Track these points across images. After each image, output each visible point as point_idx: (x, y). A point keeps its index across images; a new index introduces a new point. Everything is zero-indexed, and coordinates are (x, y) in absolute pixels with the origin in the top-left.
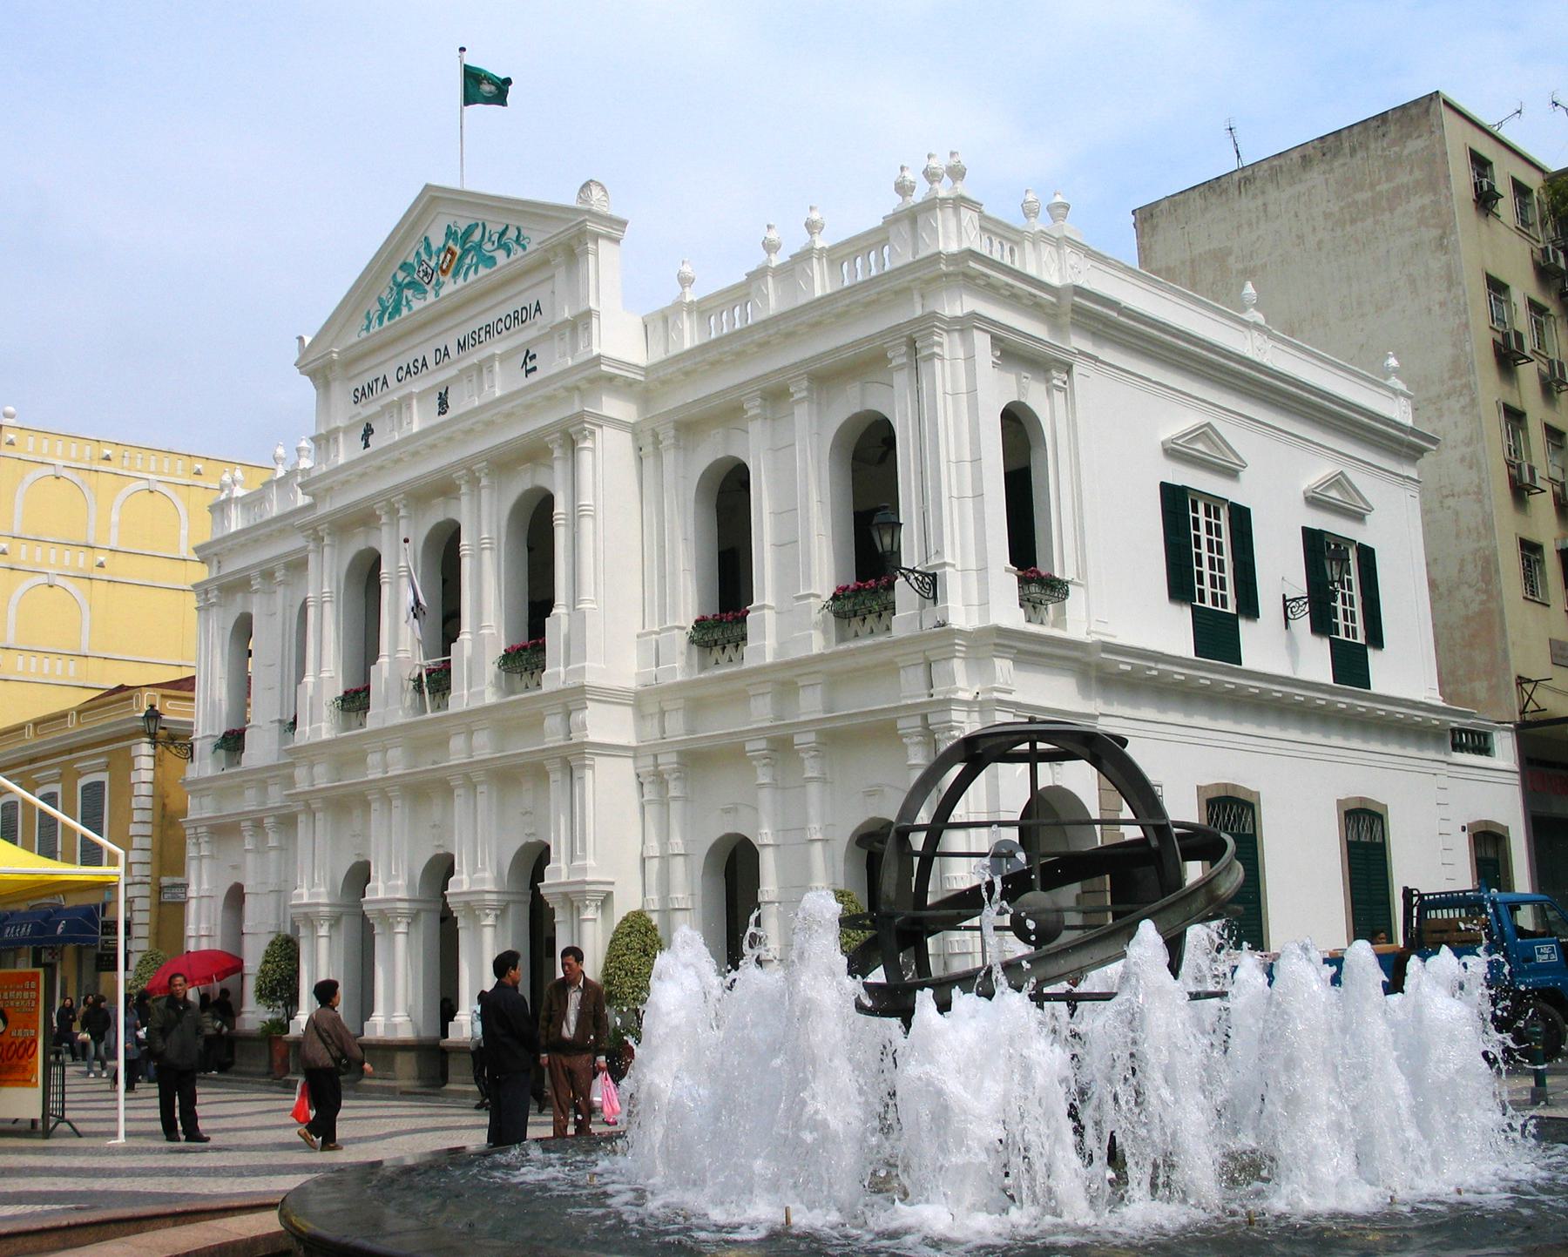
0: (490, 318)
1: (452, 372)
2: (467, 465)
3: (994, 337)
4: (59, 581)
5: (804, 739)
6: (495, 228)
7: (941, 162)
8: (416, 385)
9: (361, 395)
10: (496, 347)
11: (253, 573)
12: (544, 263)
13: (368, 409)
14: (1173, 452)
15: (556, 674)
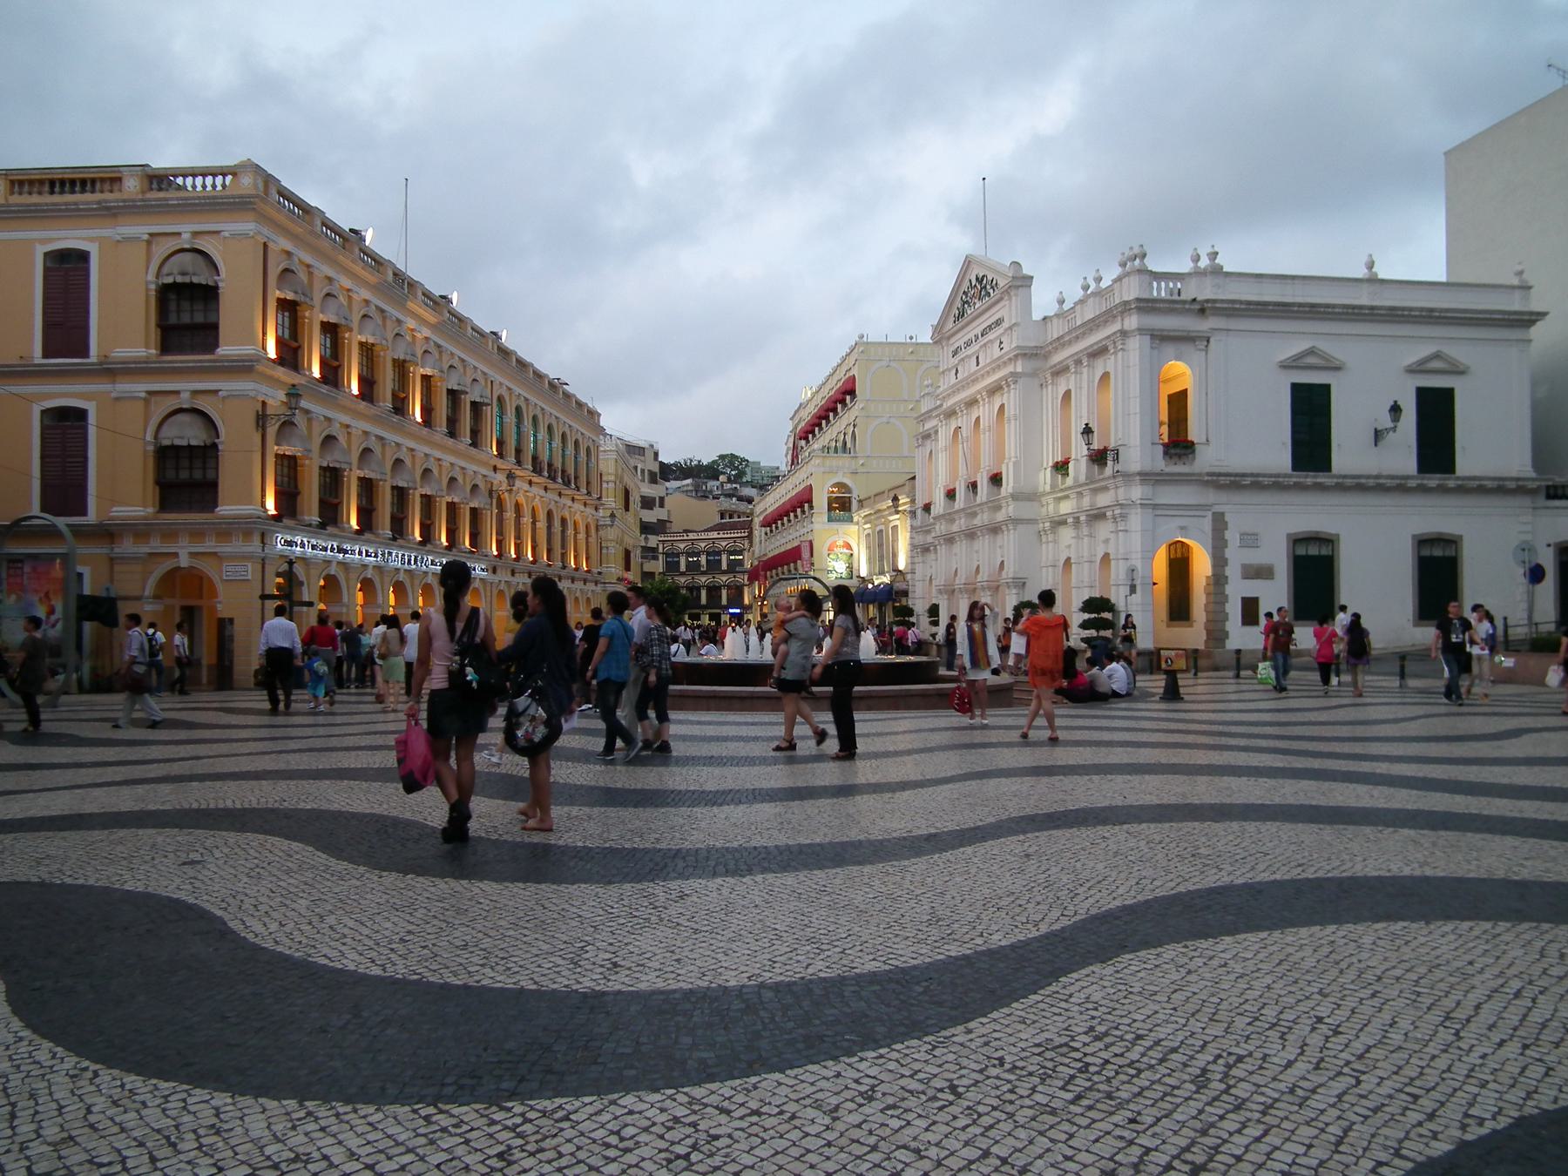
0: (989, 323)
1: (977, 347)
2: (979, 392)
3: (1153, 336)
4: (892, 420)
5: (1083, 518)
6: (990, 278)
7: (1137, 250)
8: (970, 350)
9: (955, 353)
10: (991, 336)
11: (932, 432)
12: (1001, 299)
13: (956, 360)
14: (1286, 366)
15: (1008, 486)
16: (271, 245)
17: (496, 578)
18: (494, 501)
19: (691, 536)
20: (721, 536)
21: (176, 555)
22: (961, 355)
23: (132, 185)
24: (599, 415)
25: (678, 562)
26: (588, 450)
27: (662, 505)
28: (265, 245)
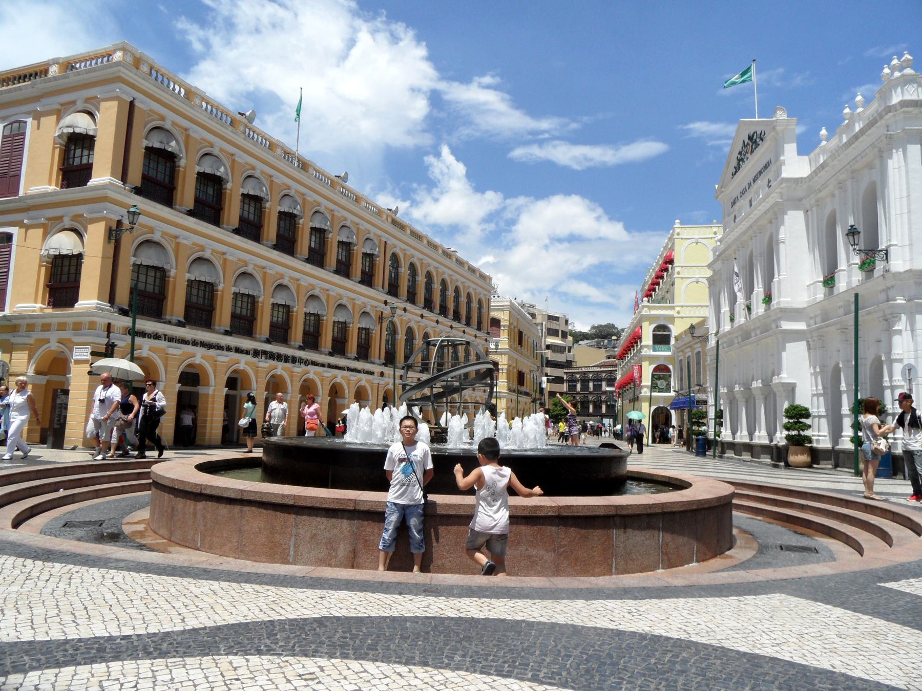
6: (759, 133)
16: (137, 103)
17: (383, 381)
18: (385, 325)
19: (584, 370)
20: (603, 369)
21: (48, 341)
22: (738, 204)
23: (54, 70)
24: (490, 279)
25: (575, 386)
26: (480, 302)
27: (569, 351)
28: (132, 104)
